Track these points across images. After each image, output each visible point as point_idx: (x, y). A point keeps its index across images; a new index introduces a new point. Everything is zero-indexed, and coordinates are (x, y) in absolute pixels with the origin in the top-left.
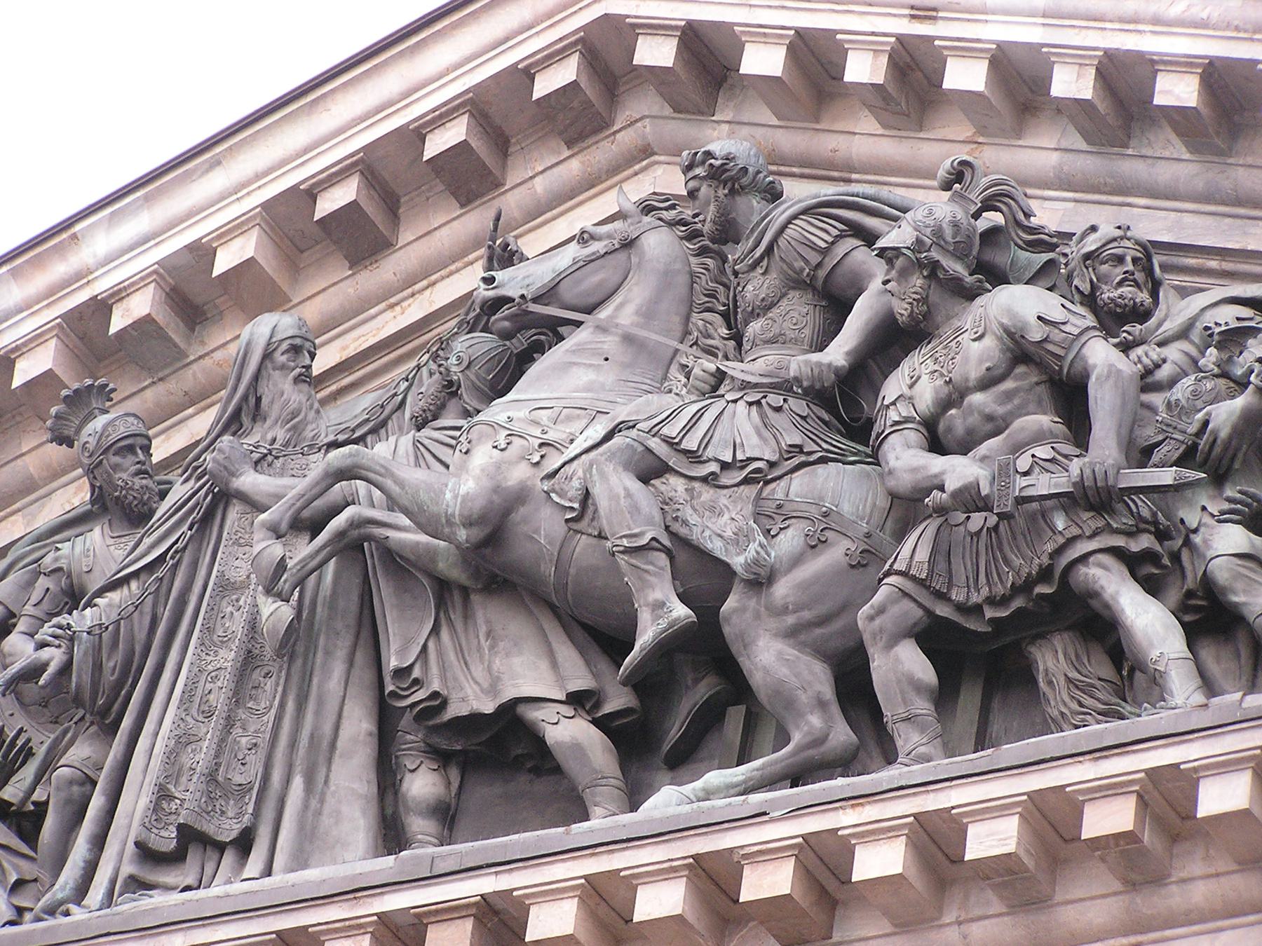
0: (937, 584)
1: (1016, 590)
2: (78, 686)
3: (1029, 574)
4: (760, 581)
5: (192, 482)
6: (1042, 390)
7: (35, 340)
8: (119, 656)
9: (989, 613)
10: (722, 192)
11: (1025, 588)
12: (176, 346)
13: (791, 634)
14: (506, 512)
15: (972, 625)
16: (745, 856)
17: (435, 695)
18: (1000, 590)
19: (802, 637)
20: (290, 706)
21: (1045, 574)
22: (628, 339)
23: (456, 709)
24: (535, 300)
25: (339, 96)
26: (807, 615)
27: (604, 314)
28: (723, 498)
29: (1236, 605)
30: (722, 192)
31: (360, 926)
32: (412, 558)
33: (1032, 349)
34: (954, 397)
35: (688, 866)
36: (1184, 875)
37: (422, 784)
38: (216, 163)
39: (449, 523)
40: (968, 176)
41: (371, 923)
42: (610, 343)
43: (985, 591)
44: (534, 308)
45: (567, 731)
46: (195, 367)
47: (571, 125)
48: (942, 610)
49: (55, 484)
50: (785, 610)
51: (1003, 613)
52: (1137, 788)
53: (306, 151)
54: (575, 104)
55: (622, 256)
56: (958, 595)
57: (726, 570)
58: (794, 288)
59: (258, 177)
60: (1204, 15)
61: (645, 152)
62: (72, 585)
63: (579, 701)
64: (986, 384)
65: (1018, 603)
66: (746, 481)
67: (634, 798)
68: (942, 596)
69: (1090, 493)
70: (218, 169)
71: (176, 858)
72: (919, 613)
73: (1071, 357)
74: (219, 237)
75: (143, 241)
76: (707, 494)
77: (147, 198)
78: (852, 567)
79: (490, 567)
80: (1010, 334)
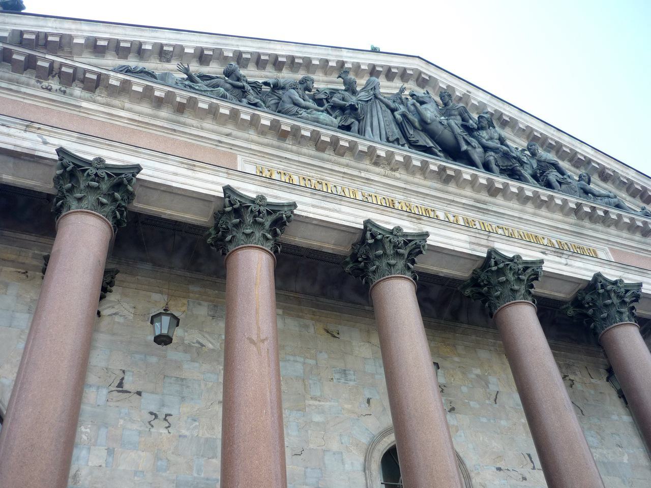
1: (505, 166)
7: (333, 61)
11: (507, 166)
21: (511, 166)
38: (363, 54)
51: (503, 168)
64: (496, 139)
65: (505, 168)
71: (393, 142)
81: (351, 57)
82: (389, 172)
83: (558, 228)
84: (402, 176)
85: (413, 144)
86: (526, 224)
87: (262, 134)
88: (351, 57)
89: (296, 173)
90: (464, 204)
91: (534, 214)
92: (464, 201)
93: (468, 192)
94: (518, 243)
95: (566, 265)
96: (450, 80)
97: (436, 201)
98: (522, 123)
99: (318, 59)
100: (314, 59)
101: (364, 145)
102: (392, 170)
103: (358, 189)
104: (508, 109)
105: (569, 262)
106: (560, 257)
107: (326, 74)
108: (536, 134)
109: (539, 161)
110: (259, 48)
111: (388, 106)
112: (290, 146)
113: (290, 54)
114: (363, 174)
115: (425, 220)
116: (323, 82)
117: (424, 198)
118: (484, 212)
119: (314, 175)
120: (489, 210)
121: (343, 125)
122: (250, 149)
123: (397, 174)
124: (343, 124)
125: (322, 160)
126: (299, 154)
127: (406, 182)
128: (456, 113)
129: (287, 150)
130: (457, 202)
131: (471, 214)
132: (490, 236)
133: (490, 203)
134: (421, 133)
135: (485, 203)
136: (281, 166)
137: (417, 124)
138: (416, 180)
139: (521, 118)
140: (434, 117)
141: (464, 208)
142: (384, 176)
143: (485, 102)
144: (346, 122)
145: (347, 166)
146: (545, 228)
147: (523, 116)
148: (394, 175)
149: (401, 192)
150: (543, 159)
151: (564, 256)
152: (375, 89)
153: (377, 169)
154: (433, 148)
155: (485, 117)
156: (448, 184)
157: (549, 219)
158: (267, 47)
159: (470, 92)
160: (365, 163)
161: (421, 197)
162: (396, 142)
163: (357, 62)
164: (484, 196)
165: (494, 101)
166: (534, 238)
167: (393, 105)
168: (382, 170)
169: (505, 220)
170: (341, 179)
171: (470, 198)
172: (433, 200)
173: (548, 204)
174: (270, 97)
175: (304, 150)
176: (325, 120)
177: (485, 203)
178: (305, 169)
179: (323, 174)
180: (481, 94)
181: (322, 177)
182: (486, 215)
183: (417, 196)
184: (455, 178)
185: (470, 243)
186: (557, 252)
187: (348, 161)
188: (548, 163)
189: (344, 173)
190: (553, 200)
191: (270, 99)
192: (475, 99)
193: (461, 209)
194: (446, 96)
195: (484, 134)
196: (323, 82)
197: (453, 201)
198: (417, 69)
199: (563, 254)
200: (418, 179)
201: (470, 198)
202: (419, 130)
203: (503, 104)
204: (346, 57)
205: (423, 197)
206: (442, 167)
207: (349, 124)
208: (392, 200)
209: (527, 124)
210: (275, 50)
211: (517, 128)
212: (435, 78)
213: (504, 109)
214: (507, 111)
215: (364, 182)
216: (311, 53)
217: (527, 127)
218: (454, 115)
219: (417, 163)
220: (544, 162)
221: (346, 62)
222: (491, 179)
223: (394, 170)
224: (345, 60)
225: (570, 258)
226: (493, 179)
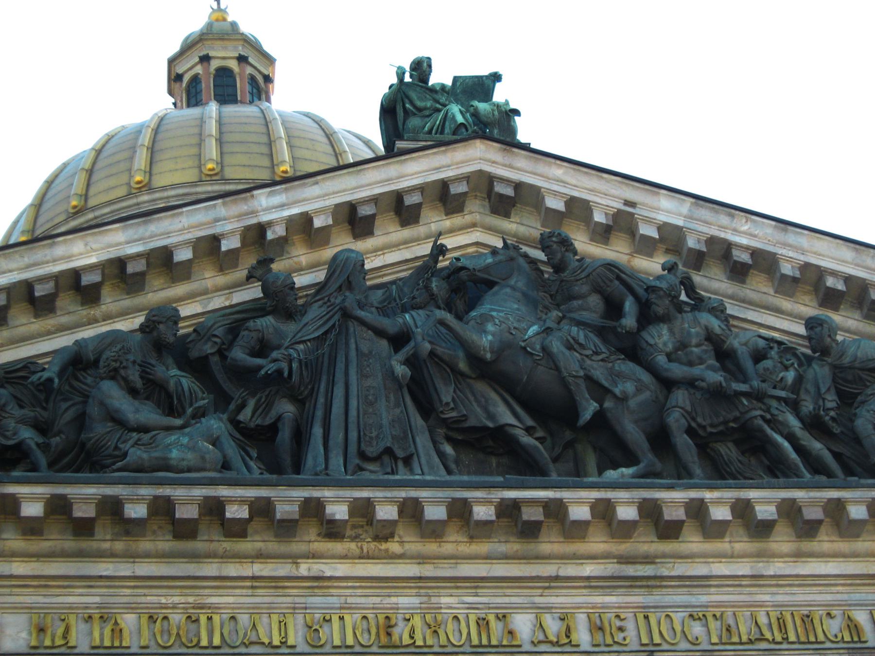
0: (694, 414)
4: (623, 399)
5: (323, 309)
6: (713, 353)
7: (232, 232)
9: (709, 429)
10: (563, 249)
11: (725, 423)
13: (636, 422)
15: (701, 432)
17: (464, 416)
18: (715, 421)
21: (735, 420)
22: (525, 295)
23: (472, 422)
24: (479, 271)
25: (370, 171)
27: (512, 282)
28: (595, 365)
29: (803, 445)
30: (563, 249)
34: (683, 346)
36: (820, 539)
37: (448, 449)
39: (484, 349)
42: (518, 295)
43: (709, 421)
44: (477, 273)
45: (526, 439)
46: (285, 261)
48: (693, 425)
49: (215, 294)
51: (714, 430)
53: (355, 188)
56: (699, 420)
57: (607, 391)
59: (334, 193)
60: (756, 233)
61: (474, 225)
62: (263, 338)
63: (529, 430)
64: (698, 345)
65: (721, 428)
67: (600, 473)
68: (694, 419)
72: (686, 424)
76: (588, 362)
77: (286, 189)
79: (487, 370)
80: (707, 328)
81: (282, 206)
82: (370, 546)
84: (407, 546)
85: (456, 426)
86: (778, 586)
87: (33, 534)
88: (282, 206)
89: (131, 608)
90: (588, 578)
91: (798, 555)
92: (589, 569)
96: (574, 182)
97: (508, 587)
98: (790, 260)
99: (186, 243)
100: (179, 245)
101: (291, 501)
102: (377, 538)
103: (294, 608)
104: (745, 228)
107: (221, 269)
109: (838, 370)
110: (29, 267)
111: (380, 333)
112: (106, 545)
113: (112, 256)
114: (304, 569)
116: (218, 289)
117: (476, 587)
118: (648, 587)
119: (176, 599)
120: (662, 578)
121: (257, 426)
122: (11, 577)
123: (394, 547)
124: (259, 422)
125: (194, 557)
126: (132, 556)
127: (422, 559)
128: (585, 289)
129: (101, 555)
131: (613, 599)
133: (664, 556)
134: (481, 387)
135: (648, 559)
136: (92, 598)
137: (462, 366)
138: (448, 548)
139: (785, 245)
140: (508, 334)
142: (360, 558)
143: (680, 222)
144: (266, 415)
145: (260, 556)
147: (792, 237)
148: (387, 550)
149: (410, 588)
150: (846, 360)
152: (350, 283)
153: (338, 547)
154: (507, 428)
155: (661, 289)
156: (537, 537)
157: (844, 556)
158: (48, 258)
159: (632, 204)
160: (306, 538)
161: (467, 588)
162: (386, 459)
163: (302, 214)
164: (646, 543)
165: (704, 213)
166: (798, 622)
167: (390, 325)
168: (353, 546)
169: (713, 590)
170: (250, 592)
171: (606, 556)
172: (502, 588)
174: (65, 400)
175: (145, 545)
176: (183, 460)
177: (648, 559)
178: (154, 591)
179: (202, 592)
180: (665, 202)
181: (200, 600)
182: (656, 591)
183: (457, 588)
187: (260, 545)
189: (254, 578)
190: (845, 508)
191: (64, 405)
192: (649, 221)
193: (585, 591)
194: (555, 246)
195: (661, 338)
196: (218, 289)
197: (557, 578)
198: (480, 171)
200: (455, 542)
201: (606, 556)
202: (471, 378)
204: (268, 209)
205: (471, 588)
207: (273, 421)
208: (387, 617)
209: (802, 258)
210: (69, 258)
211: (778, 275)
212: (532, 187)
214: (744, 233)
215: (309, 588)
216: (168, 234)
217: (806, 267)
219: (435, 512)
220: (850, 368)
221: (270, 224)
223: (386, 539)
224: (265, 218)
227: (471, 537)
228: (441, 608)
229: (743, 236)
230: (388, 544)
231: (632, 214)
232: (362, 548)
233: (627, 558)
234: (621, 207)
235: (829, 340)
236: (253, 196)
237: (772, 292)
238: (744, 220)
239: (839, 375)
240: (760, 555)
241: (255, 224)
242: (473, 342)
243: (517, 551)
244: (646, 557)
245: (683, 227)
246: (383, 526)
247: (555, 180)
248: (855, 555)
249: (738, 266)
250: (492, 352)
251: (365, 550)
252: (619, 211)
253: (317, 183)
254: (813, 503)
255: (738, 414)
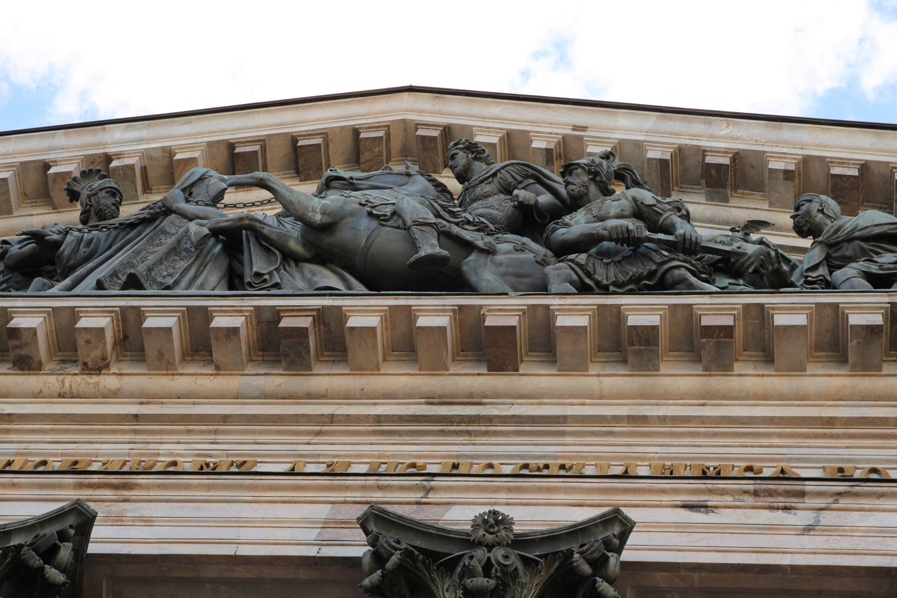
2: (64, 250)
3: (642, 273)
8: (88, 250)
12: (136, 191)
13: (503, 275)
14: (342, 218)
16: (489, 310)
18: (622, 278)
19: (507, 278)
20: (193, 271)
26: (511, 270)
31: (241, 311)
32: (274, 237)
33: (645, 209)
35: (453, 310)
39: (313, 210)
40: (612, 158)
41: (248, 311)
47: (370, 160)
50: (501, 264)
52: (735, 312)
54: (376, 150)
55: (406, 178)
58: (502, 193)
66: (478, 230)
68: (589, 275)
69: (687, 242)
70: (188, 125)
73: (665, 216)
74: (181, 149)
75: (140, 141)
78: (537, 262)
83: (830, 422)
84: (126, 379)
93: (398, 377)
94: (566, 490)
95: (808, 529)
97: (261, 432)
104: (725, 132)
105: (828, 518)
106: (786, 509)
108: (836, 171)
115: (148, 487)
117: (216, 432)
123: (108, 381)
130: (349, 419)
132: (432, 489)
135: (471, 399)
141: (382, 433)
142: (60, 396)
143: (641, 138)
146: (769, 435)
148: (97, 384)
151: (809, 502)
153: (31, 381)
159: (584, 128)
161: (202, 432)
163: (163, 149)
168: (52, 379)
169: (568, 440)
171: (409, 395)
172: (253, 432)
173: (763, 343)
183: (189, 432)
184: (334, 342)
185: (326, 524)
186: (771, 493)
188: (865, 239)
193: (373, 439)
197: (332, 419)
199: (802, 494)
200: (195, 378)
201: (409, 395)
203: (705, 122)
205: (209, 432)
206: (267, 315)
209: (800, 152)
212: (463, 127)
213: (712, 137)
218: (486, 196)
221: (119, 155)
222: (473, 306)
225: (844, 502)
226: (481, 307)
227: (218, 368)
228: (158, 454)
229: (720, 142)
230: (101, 377)
231: (583, 137)
232: (63, 382)
233: (440, 397)
234: (570, 132)
235: (820, 215)
236: (105, 129)
237: (767, 207)
238: (725, 125)
239: (834, 255)
240: (644, 396)
241: (99, 155)
242: (299, 203)
243: (280, 385)
244: (471, 395)
245: (643, 141)
246: (88, 342)
247: (491, 118)
248: (802, 397)
249: (713, 172)
250: (323, 213)
251: (67, 384)
252: (565, 138)
253: (190, 123)
254: (719, 310)
255: (654, 267)
